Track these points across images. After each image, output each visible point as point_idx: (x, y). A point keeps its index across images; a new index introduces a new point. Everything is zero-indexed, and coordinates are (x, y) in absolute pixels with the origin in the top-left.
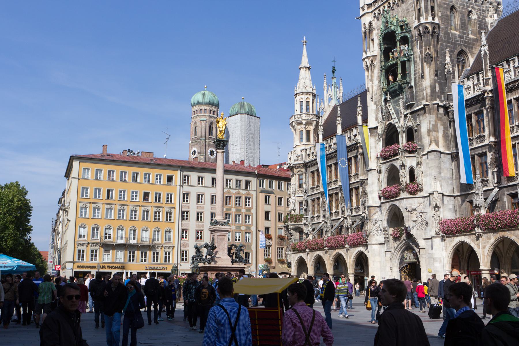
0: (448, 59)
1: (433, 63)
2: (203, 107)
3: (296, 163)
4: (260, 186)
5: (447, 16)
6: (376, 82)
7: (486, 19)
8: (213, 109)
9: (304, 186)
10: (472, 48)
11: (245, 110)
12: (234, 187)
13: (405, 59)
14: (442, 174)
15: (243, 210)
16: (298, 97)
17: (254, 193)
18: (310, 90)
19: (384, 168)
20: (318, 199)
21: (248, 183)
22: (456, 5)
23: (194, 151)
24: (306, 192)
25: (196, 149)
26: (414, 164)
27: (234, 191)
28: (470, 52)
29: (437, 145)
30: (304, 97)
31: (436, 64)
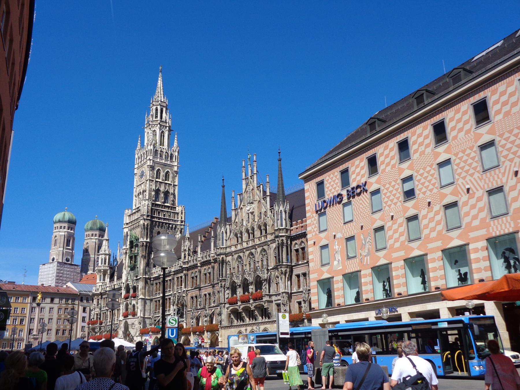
2: (63, 225)
6: (127, 261)
11: (97, 226)
18: (107, 252)
19: (125, 303)
24: (100, 309)
26: (135, 303)
30: (103, 256)
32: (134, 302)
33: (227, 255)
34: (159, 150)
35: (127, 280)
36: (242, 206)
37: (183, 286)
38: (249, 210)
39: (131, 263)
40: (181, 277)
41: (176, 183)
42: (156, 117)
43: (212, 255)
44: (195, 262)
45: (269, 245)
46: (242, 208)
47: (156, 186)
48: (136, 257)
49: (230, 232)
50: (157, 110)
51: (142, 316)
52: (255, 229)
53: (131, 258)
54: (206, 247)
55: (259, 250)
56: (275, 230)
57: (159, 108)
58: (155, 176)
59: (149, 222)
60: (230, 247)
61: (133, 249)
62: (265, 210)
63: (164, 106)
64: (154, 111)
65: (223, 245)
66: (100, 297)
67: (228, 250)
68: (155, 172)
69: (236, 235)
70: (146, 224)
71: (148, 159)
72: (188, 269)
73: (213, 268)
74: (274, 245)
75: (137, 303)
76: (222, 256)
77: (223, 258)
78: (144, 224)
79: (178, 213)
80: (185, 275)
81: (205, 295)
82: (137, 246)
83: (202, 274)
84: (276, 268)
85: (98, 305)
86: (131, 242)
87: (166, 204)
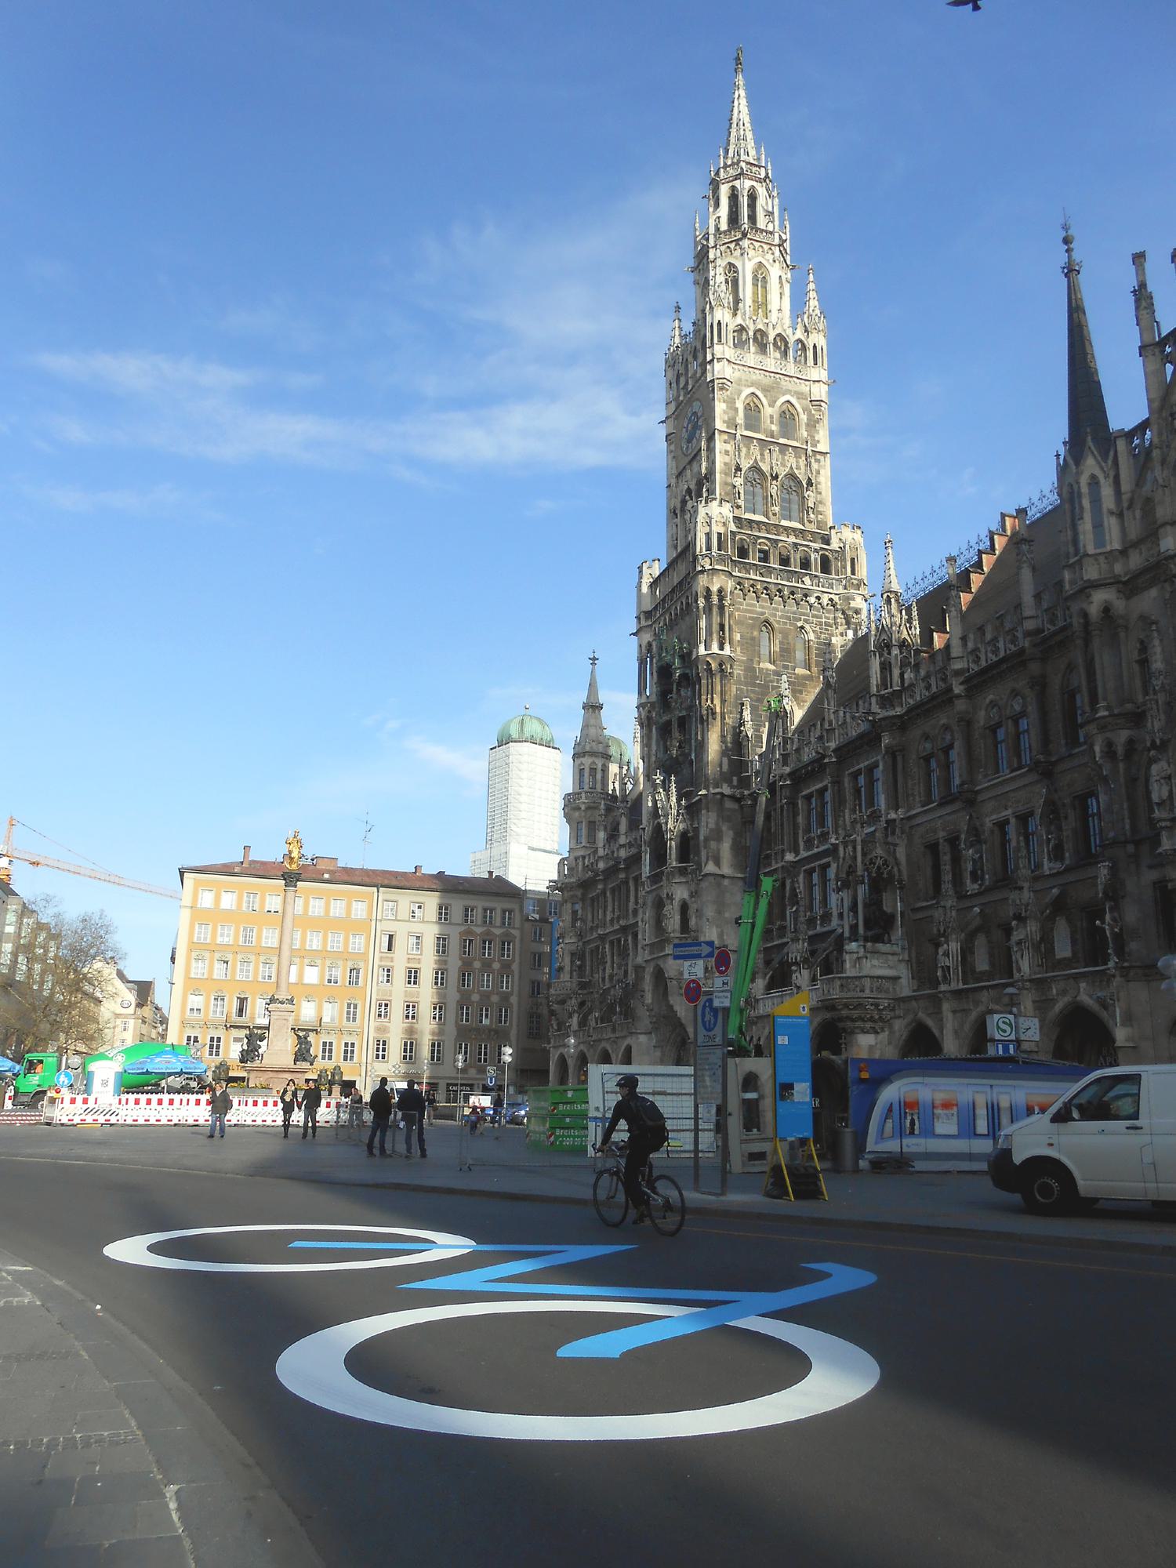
5: (753, 639)
9: (578, 924)
10: (801, 692)
13: (684, 713)
14: (727, 915)
15: (496, 966)
16: (578, 761)
20: (597, 947)
22: (771, 619)
24: (580, 936)
26: (686, 895)
27: (479, 930)
29: (718, 863)
31: (723, 724)
32: (680, 893)
37: (882, 801)
40: (871, 769)
41: (823, 447)
47: (748, 455)
50: (734, 197)
58: (740, 419)
59: (730, 585)
66: (579, 893)
68: (740, 405)
70: (715, 589)
72: (901, 724)
78: (708, 590)
81: (1002, 825)
85: (573, 926)
86: (664, 672)
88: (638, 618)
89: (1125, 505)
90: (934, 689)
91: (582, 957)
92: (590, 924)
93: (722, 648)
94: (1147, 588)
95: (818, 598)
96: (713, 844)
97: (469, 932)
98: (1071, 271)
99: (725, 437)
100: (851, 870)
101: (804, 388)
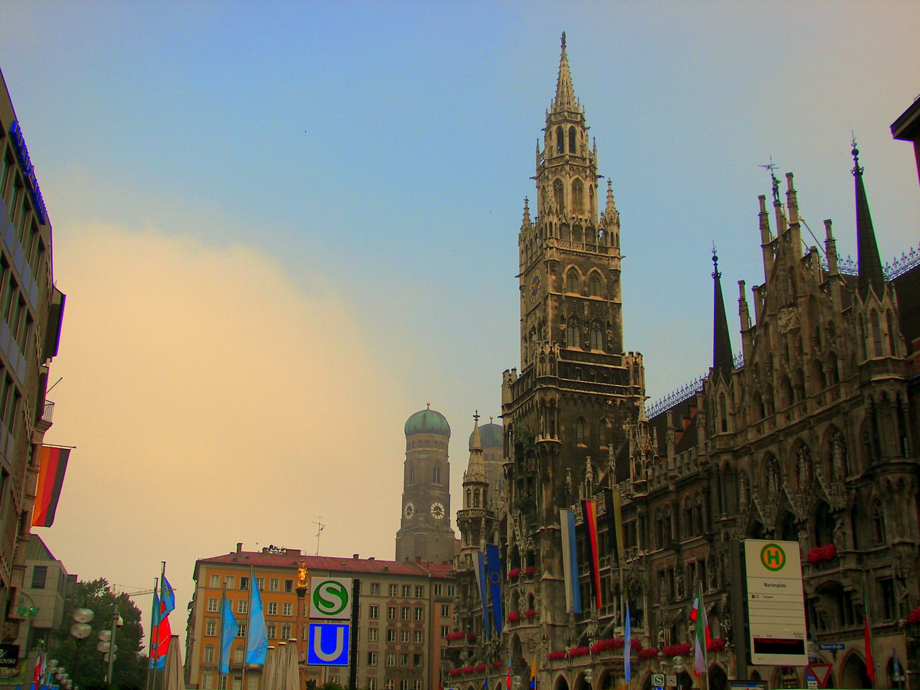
0: (569, 479)
1: (551, 484)
2: (423, 437)
3: (459, 571)
4: (436, 593)
5: (573, 429)
7: (624, 427)
8: (438, 438)
10: (603, 462)
12: (400, 596)
15: (412, 625)
17: (426, 603)
21: (419, 589)
23: (410, 508)
24: (470, 609)
25: (411, 505)
27: (399, 601)
28: (600, 466)
29: (551, 571)
30: (471, 487)
32: (530, 589)
33: (737, 454)
34: (571, 223)
35: (514, 539)
36: (767, 319)
38: (785, 326)
39: (521, 496)
40: (634, 523)
42: (561, 149)
43: (702, 459)
44: (663, 483)
45: (846, 414)
46: (766, 326)
48: (530, 481)
49: (743, 390)
51: (550, 622)
52: (806, 374)
53: (520, 484)
54: (687, 441)
55: (820, 430)
56: (861, 367)
57: (566, 127)
60: (744, 432)
61: (524, 464)
62: (828, 319)
63: (577, 123)
64: (554, 136)
65: (724, 428)
66: (468, 579)
67: (740, 442)
68: (564, 276)
69: (757, 396)
71: (545, 246)
72: (644, 501)
73: (707, 492)
74: (861, 413)
75: (538, 590)
76: (725, 457)
77: (727, 463)
79: (625, 373)
80: (642, 518)
82: (530, 454)
83: (681, 512)
84: (869, 476)
86: (519, 447)
87: (593, 351)
88: (503, 407)
89: (736, 410)
90: (662, 484)
91: (471, 623)
92: (475, 601)
93: (552, 438)
94: (745, 456)
95: (614, 401)
96: (548, 560)
97: (393, 602)
98: (716, 276)
99: (555, 298)
100: (617, 587)
101: (605, 262)
